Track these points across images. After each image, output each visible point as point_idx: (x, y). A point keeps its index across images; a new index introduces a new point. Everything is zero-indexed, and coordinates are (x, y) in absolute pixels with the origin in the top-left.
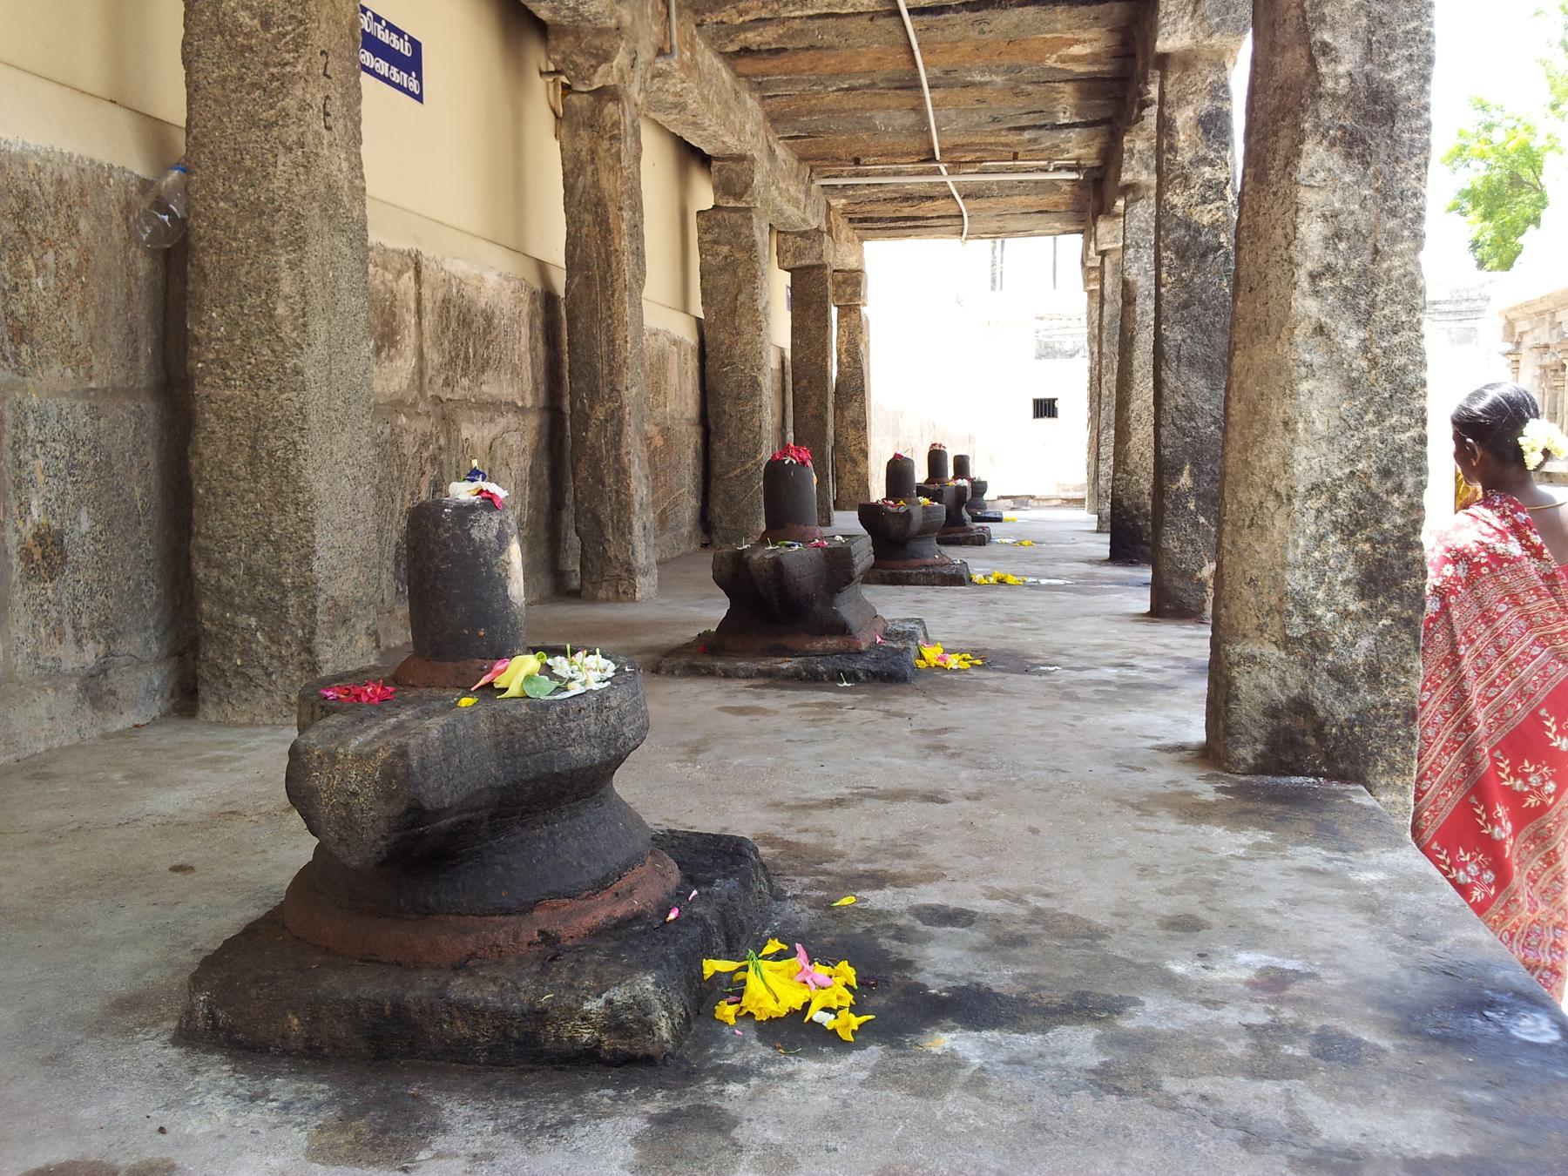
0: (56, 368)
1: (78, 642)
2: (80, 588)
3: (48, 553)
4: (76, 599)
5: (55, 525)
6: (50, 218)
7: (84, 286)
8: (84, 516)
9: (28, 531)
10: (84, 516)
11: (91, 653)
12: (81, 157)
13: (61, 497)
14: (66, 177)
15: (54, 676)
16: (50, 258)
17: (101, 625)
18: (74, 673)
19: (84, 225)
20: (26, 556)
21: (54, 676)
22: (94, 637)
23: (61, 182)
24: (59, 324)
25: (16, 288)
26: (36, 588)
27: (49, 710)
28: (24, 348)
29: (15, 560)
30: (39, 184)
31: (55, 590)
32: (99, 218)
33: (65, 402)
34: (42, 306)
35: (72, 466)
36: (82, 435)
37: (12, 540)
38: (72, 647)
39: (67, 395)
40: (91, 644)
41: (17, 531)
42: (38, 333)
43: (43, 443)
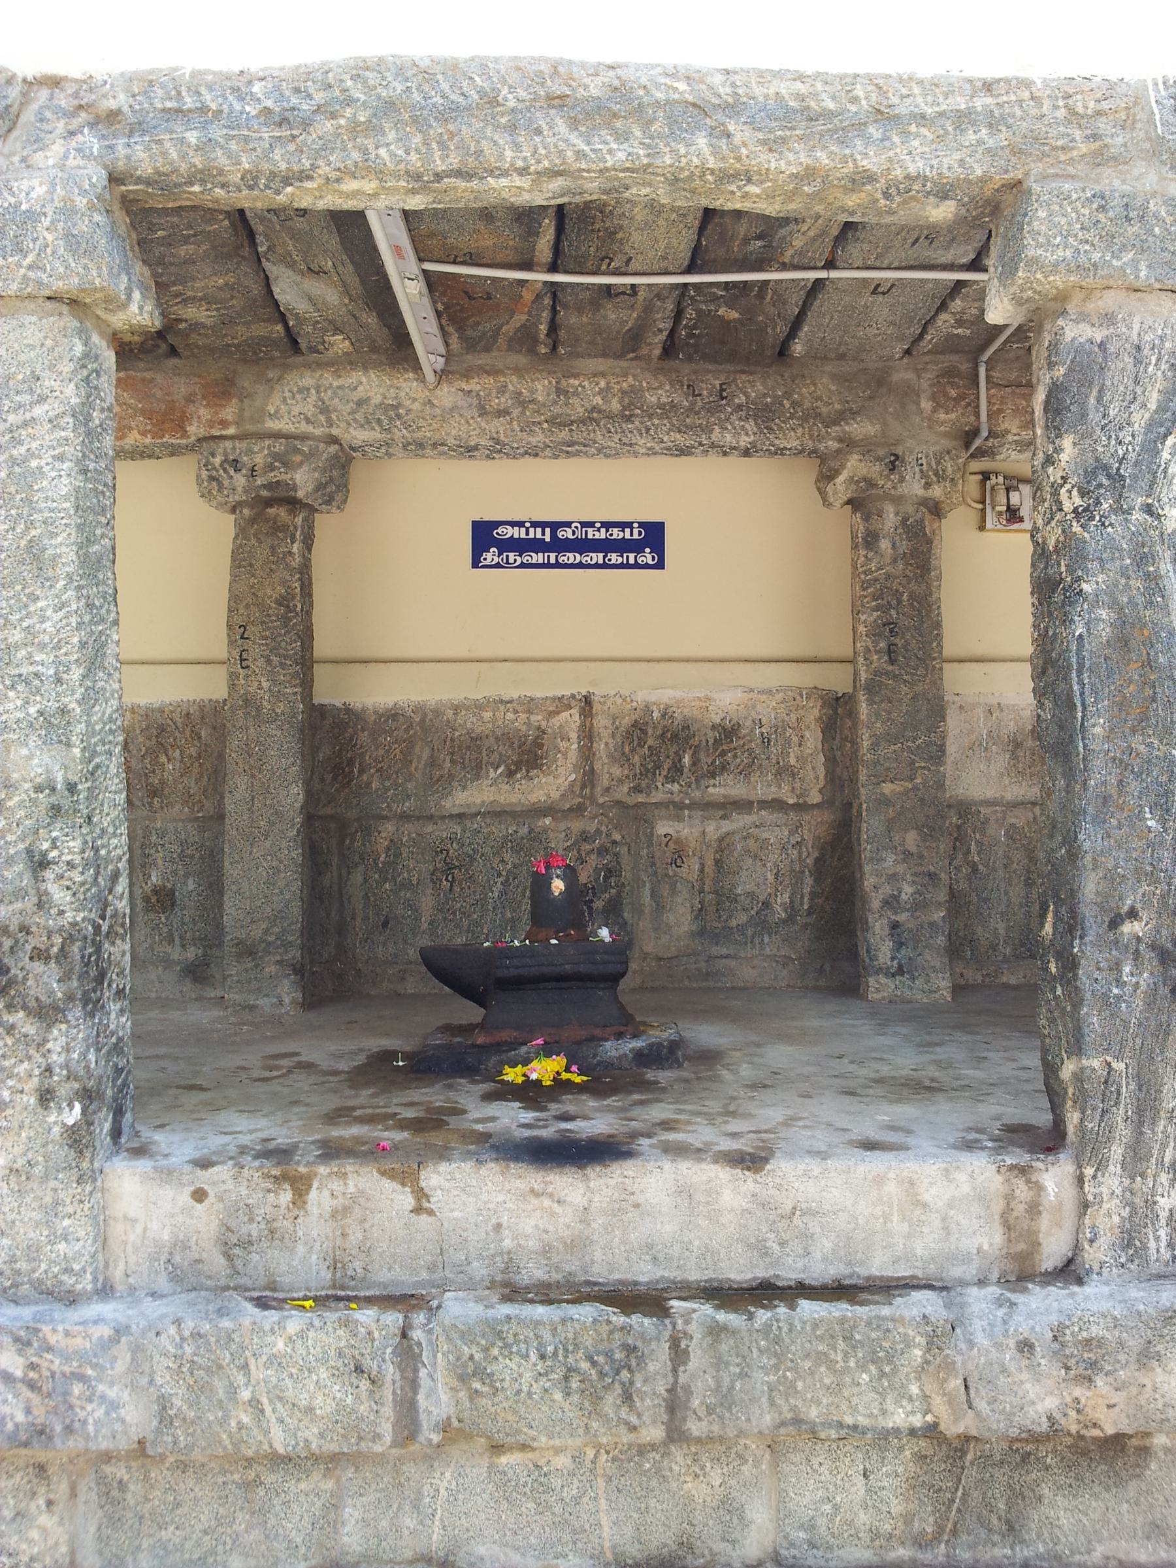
0: (178, 807)
1: (183, 946)
4: (183, 924)
5: (169, 886)
8: (190, 882)
9: (148, 888)
10: (190, 882)
11: (191, 953)
15: (167, 962)
17: (200, 939)
18: (179, 963)
19: (203, 733)
20: (146, 899)
21: (167, 962)
23: (188, 714)
26: (152, 916)
27: (159, 977)
32: (214, 728)
35: (182, 856)
36: (190, 840)
38: (178, 949)
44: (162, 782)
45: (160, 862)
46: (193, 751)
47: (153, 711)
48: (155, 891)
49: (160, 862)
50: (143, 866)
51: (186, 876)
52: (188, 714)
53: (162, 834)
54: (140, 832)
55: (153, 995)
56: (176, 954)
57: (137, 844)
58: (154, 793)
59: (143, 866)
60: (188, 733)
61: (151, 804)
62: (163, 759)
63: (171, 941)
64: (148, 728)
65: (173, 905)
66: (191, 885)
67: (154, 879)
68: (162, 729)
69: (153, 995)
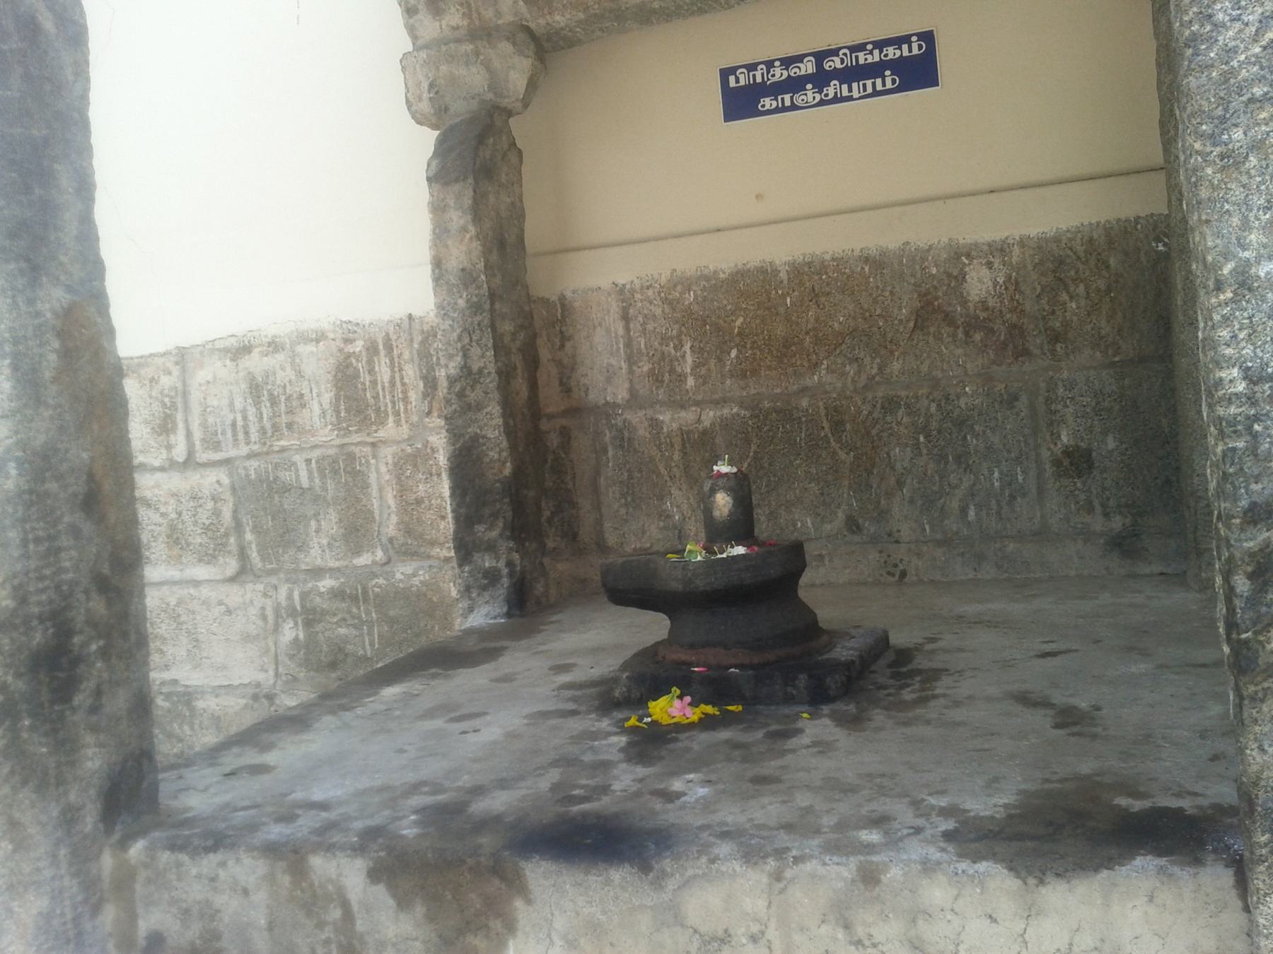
1: (1106, 515)
2: (1108, 483)
3: (1077, 462)
4: (1104, 489)
6: (1081, 267)
7: (1112, 300)
9: (1058, 450)
11: (1117, 523)
12: (1109, 222)
13: (1090, 430)
14: (1095, 236)
16: (1081, 289)
19: (1112, 261)
20: (1057, 463)
22: (1121, 513)
23: (1091, 240)
24: (1089, 327)
25: (1053, 312)
28: (1058, 346)
29: (1048, 466)
30: (1071, 249)
31: (1084, 483)
32: (1126, 254)
33: (1092, 372)
34: (1075, 318)
37: (1045, 454)
39: (1095, 368)
40: (1118, 518)
41: (1049, 449)
42: (1070, 335)
43: (1072, 399)
44: (1066, 324)
45: (1070, 419)
46: (1102, 284)
47: (1047, 240)
48: (1067, 453)
49: (1070, 419)
50: (1051, 424)
51: (1105, 433)
52: (1091, 240)
53: (1070, 385)
54: (1043, 385)
55: (1072, 573)
56: (1097, 523)
57: (1041, 399)
58: (1055, 338)
59: (1051, 424)
60: (1092, 262)
61: (1053, 352)
62: (1064, 297)
63: (1090, 509)
64: (1042, 262)
65: (1091, 467)
66: (1111, 443)
67: (1064, 439)
68: (1061, 262)
69: (1072, 573)
